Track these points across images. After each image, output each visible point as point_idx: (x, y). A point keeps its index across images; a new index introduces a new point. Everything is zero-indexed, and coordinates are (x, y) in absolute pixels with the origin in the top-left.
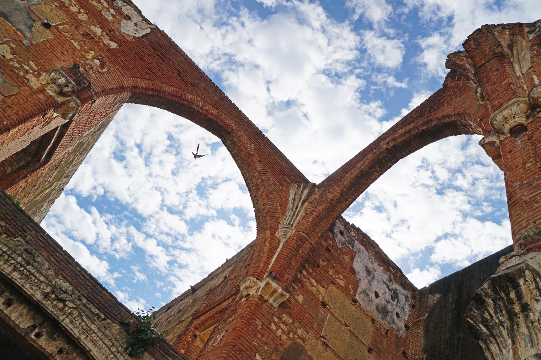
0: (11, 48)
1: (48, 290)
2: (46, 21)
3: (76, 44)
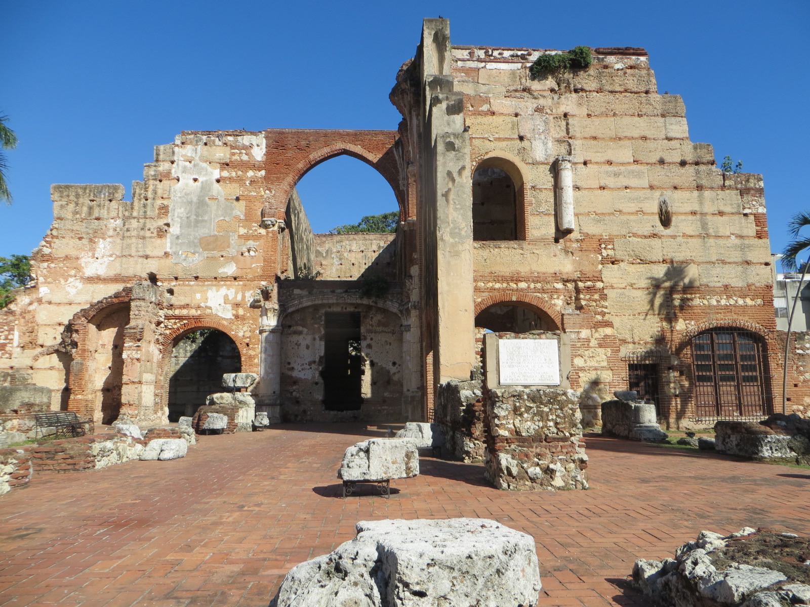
3: (253, 194)
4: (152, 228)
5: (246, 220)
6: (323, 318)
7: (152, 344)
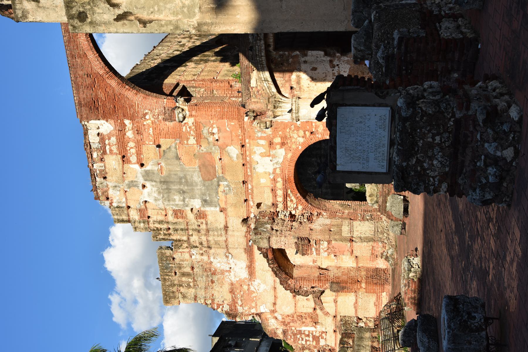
0: (187, 141)
1: (258, 41)
2: (158, 149)
4: (196, 223)
5: (180, 137)
6: (281, 53)
7: (313, 226)
